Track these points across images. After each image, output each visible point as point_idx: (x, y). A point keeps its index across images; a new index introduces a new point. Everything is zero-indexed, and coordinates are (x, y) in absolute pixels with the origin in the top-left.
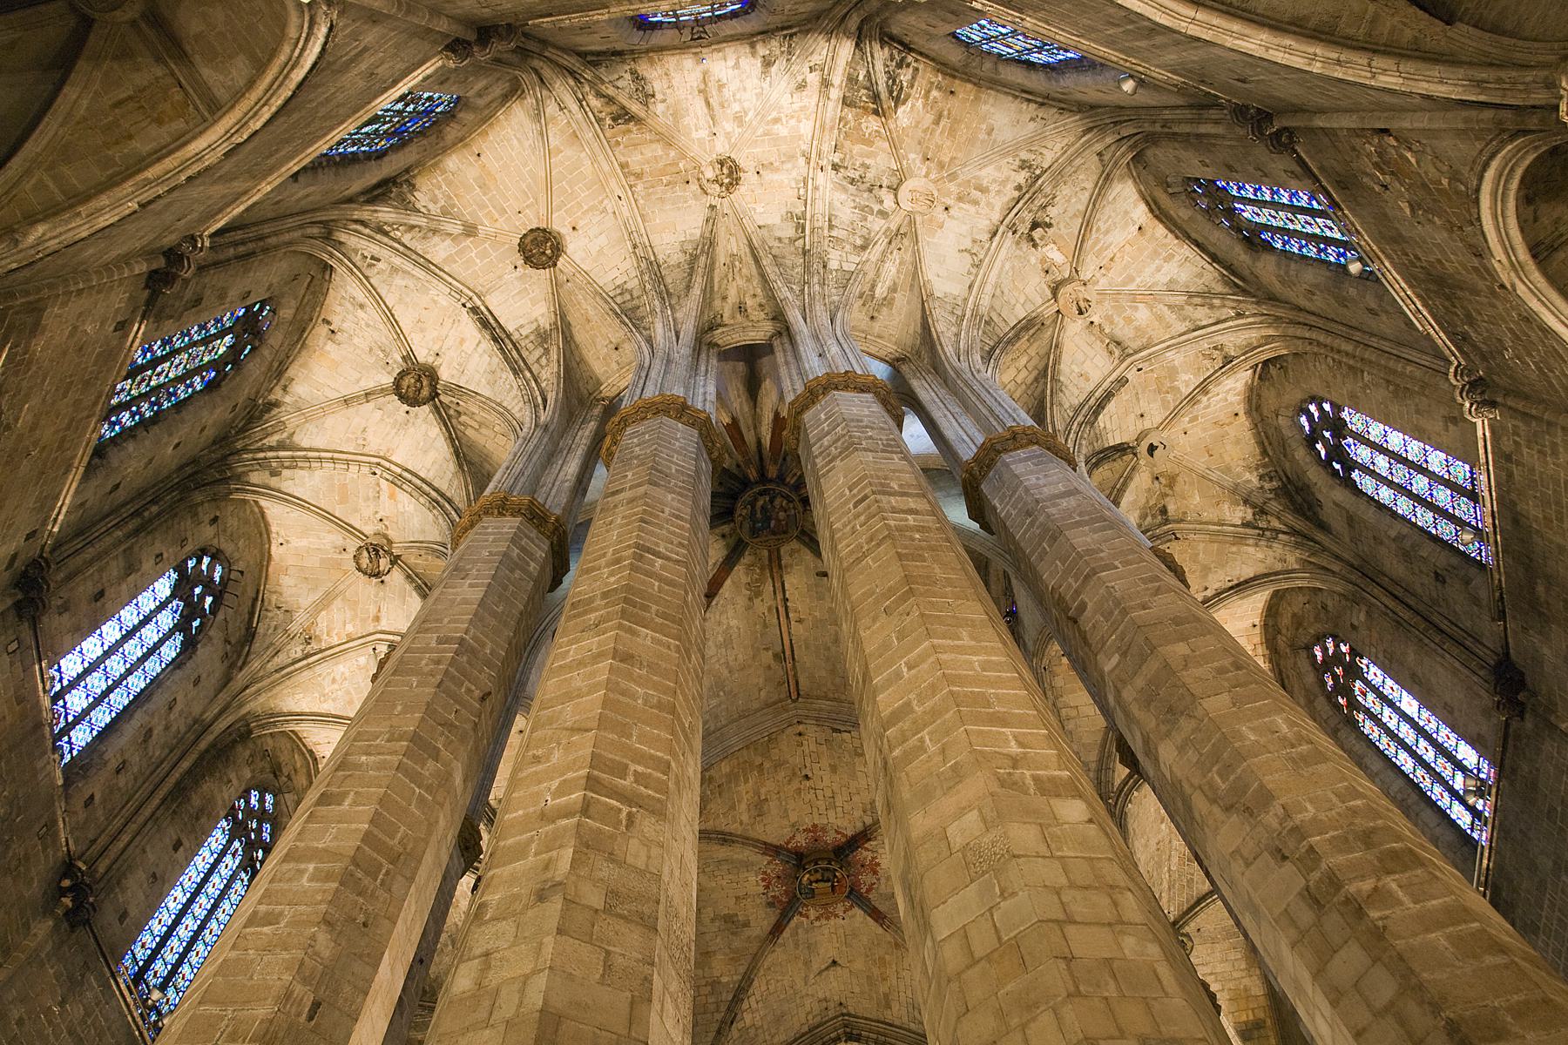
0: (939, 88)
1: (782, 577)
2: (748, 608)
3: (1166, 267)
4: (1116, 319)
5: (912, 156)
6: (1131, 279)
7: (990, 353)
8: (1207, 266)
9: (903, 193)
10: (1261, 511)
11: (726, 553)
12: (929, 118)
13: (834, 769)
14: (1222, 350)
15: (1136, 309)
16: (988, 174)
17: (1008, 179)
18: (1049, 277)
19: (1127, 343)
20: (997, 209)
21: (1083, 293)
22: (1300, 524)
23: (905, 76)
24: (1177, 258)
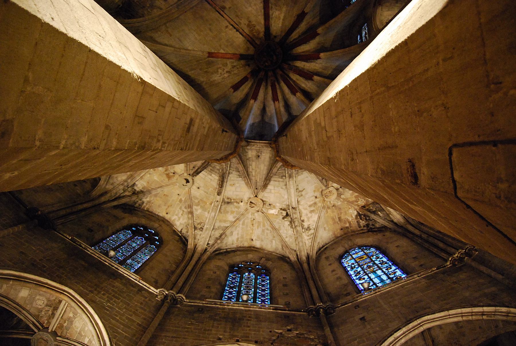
0: (347, 228)
1: (245, 38)
2: (248, 18)
3: (237, 237)
4: (236, 209)
5: (339, 203)
6: (243, 224)
7: (483, 195)
8: (226, 248)
9: (335, 191)
11: (271, 32)
12: (343, 217)
14: (200, 229)
16: (315, 217)
17: (309, 221)
18: (268, 204)
19: (226, 205)
20: (303, 211)
22: (123, 201)
23: (363, 223)
24: (235, 242)
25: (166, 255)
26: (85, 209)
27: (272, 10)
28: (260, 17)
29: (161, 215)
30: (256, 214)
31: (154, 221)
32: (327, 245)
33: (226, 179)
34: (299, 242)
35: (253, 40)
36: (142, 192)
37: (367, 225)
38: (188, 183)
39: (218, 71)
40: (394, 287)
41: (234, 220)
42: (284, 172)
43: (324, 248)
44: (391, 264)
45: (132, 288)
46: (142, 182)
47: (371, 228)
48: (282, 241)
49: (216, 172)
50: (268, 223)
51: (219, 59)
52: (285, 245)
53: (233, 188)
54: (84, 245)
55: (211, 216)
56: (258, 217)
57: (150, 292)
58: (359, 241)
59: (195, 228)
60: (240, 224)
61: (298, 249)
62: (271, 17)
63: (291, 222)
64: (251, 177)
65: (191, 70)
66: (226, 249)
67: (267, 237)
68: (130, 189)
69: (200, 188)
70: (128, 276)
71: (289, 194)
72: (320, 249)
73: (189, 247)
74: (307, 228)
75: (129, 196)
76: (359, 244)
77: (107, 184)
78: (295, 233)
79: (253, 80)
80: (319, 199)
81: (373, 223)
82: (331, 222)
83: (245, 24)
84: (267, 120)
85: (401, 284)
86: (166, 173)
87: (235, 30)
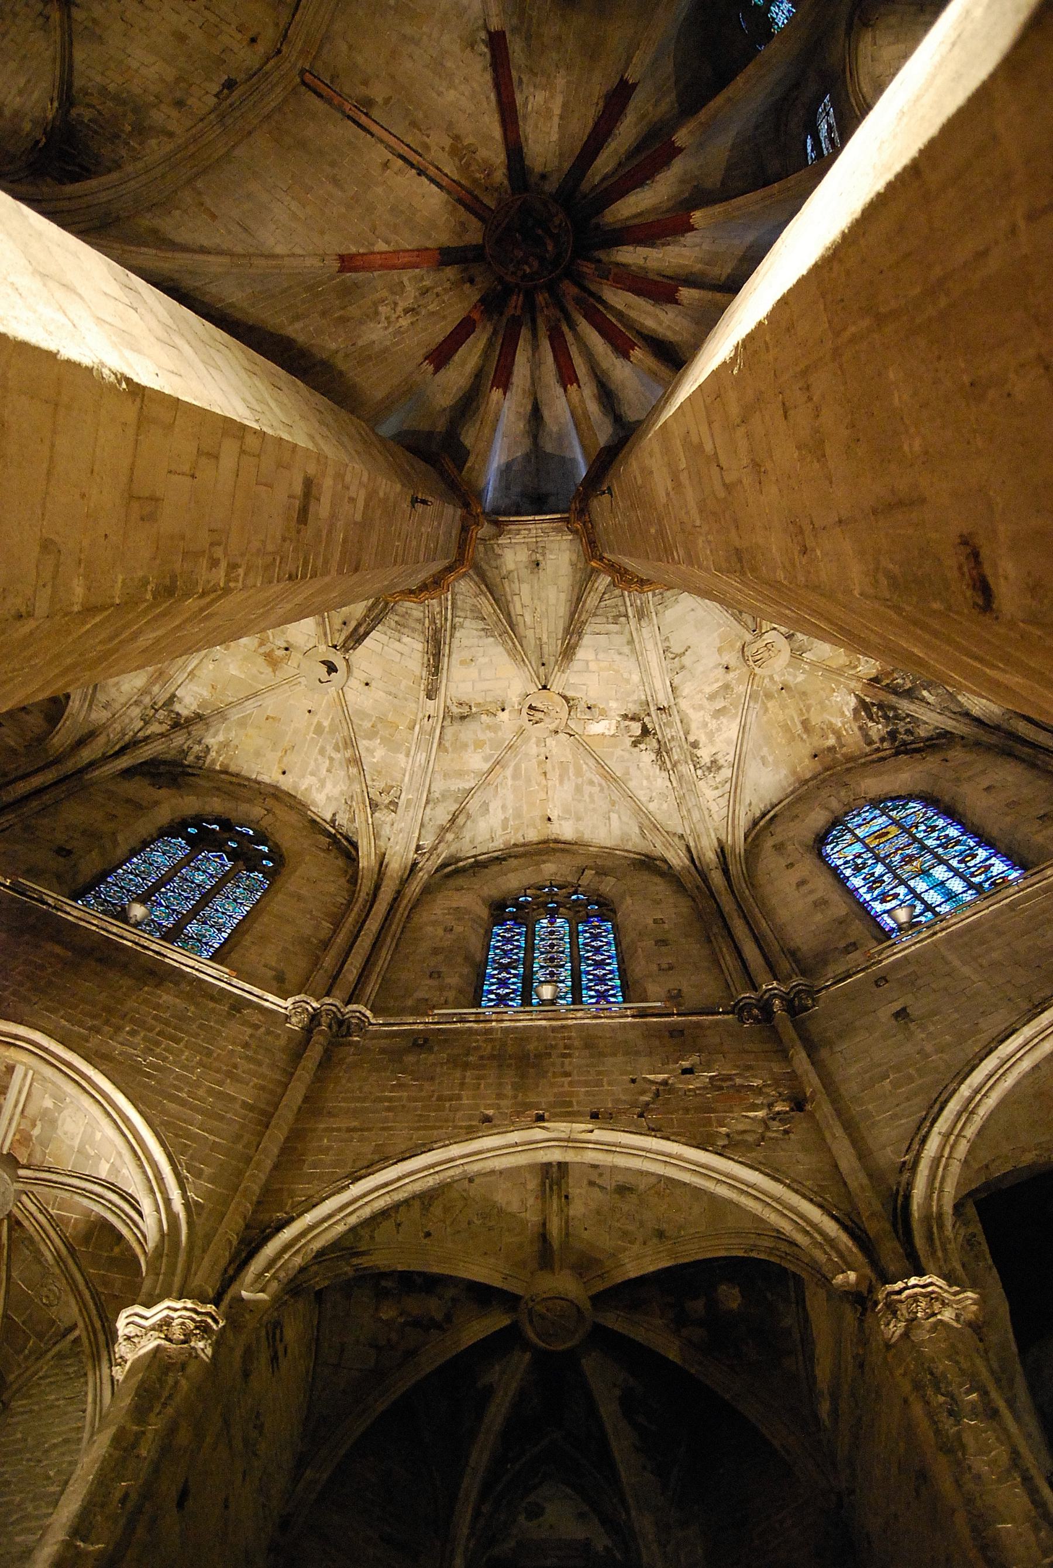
0: (832, 749)
1: (449, 193)
2: (450, 125)
3: (501, 816)
4: (490, 735)
5: (801, 678)
6: (516, 776)
10: (178, 724)
12: (815, 720)
13: (181, 38)
14: (387, 807)
15: (486, 759)
16: (730, 729)
17: (712, 741)
18: (582, 705)
19: (457, 726)
20: (690, 712)
21: (549, 724)
22: (146, 753)
23: (877, 729)
24: (499, 832)
25: (300, 898)
26: (39, 792)
27: (522, 91)
28: (486, 119)
29: (265, 778)
30: (551, 742)
31: (249, 801)
32: (777, 809)
33: (447, 647)
34: (689, 811)
35: (476, 198)
36: (199, 717)
37: (893, 735)
38: (333, 674)
39: (377, 313)
40: (986, 911)
41: (486, 767)
42: (620, 601)
43: (768, 817)
44: (972, 844)
45: (212, 1005)
46: (196, 689)
47: (904, 743)
48: (639, 810)
49: (414, 630)
50: (592, 762)
51: (376, 274)
52: (649, 824)
53: (472, 672)
54: (51, 897)
55: (417, 764)
56: (559, 748)
57: (266, 1009)
58: (872, 785)
59: (374, 806)
60: (505, 778)
61: (688, 832)
62: (521, 112)
63: (659, 752)
64: (521, 629)
65: (297, 318)
66: (474, 856)
67: (592, 806)
68: (162, 714)
69: (373, 684)
70: (195, 972)
71: (643, 668)
72: (755, 823)
73: (363, 863)
74: (709, 765)
75: (162, 735)
76: (871, 795)
77: (90, 706)
78: (675, 785)
79: (490, 329)
80: (738, 671)
81: (909, 726)
82: (781, 739)
83: (443, 148)
84: (549, 447)
85: (1008, 900)
86: (262, 650)
87: (414, 171)
